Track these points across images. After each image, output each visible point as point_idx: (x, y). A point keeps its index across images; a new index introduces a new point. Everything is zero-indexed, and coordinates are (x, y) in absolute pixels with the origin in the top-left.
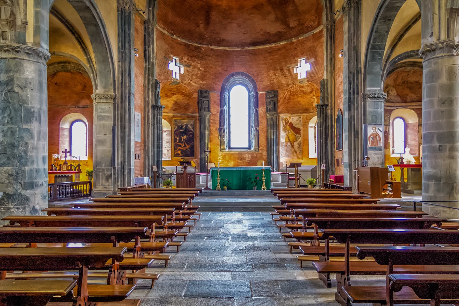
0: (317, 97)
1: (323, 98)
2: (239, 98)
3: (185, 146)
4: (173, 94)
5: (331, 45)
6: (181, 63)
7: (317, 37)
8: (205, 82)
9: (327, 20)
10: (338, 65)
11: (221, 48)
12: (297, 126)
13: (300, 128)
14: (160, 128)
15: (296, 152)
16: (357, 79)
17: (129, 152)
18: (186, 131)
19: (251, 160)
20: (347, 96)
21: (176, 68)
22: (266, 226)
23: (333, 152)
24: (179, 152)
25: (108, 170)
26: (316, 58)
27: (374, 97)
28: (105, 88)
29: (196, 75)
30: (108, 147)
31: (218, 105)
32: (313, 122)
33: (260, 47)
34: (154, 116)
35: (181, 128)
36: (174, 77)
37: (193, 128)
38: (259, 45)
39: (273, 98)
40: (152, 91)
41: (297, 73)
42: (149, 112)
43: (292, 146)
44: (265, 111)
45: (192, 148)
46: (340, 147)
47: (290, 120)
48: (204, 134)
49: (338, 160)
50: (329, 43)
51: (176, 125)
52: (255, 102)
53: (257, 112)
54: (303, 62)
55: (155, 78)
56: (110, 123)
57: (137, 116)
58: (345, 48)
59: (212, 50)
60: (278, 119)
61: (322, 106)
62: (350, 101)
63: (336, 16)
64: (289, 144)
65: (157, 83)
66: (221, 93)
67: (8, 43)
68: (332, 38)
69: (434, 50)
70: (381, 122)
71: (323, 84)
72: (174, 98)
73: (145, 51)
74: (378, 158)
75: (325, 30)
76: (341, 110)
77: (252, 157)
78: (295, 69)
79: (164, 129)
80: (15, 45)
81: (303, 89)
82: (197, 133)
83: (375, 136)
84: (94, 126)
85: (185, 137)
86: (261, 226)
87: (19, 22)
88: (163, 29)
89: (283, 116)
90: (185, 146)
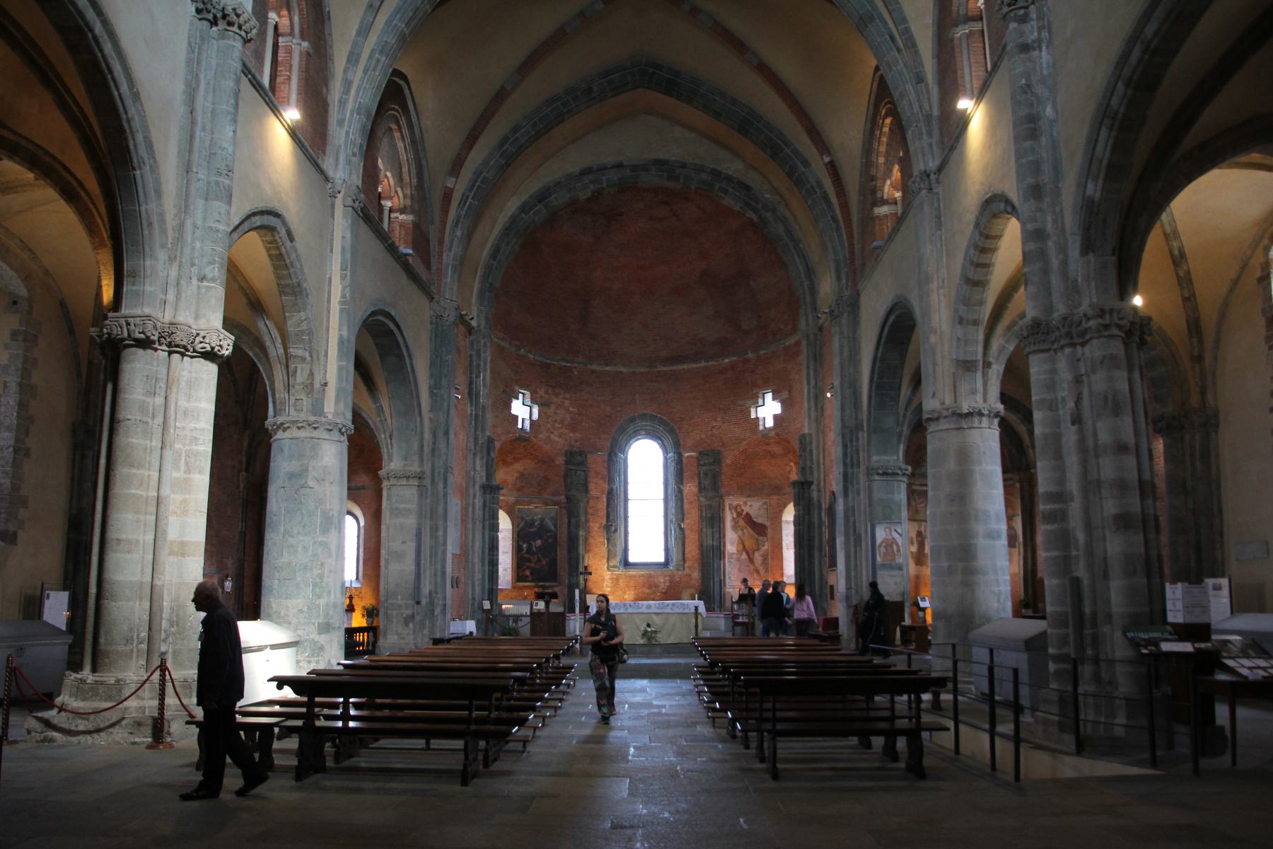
0: (796, 463)
1: (803, 469)
2: (645, 465)
3: (539, 560)
4: (516, 460)
5: (816, 371)
6: (534, 401)
7: (792, 353)
8: (578, 435)
9: (807, 325)
10: (828, 412)
11: (607, 368)
12: (759, 520)
13: (767, 523)
14: (494, 528)
15: (757, 571)
16: (857, 440)
17: (444, 573)
18: (542, 531)
19: (669, 588)
20: (841, 470)
21: (521, 410)
22: (684, 695)
23: (825, 572)
24: (528, 572)
25: (407, 607)
26: (790, 391)
27: (885, 474)
28: (405, 459)
29: (562, 422)
30: (409, 566)
31: (602, 478)
32: (789, 514)
33: (685, 366)
34: (484, 506)
35: (531, 524)
36: (520, 426)
37: (555, 526)
38: (683, 363)
39: (711, 464)
40: (482, 458)
41: (757, 418)
42: (474, 496)
43: (751, 560)
44: (695, 489)
45: (553, 563)
46: (833, 564)
47: (746, 509)
48: (577, 537)
49: (832, 587)
50: (812, 367)
51: (522, 518)
52: (677, 474)
53: (680, 491)
54: (769, 396)
55: (488, 433)
56: (411, 521)
57: (455, 505)
58: (837, 382)
59: (593, 372)
60: (720, 508)
61: (802, 484)
62: (846, 479)
63: (821, 321)
64: (744, 556)
65: (490, 441)
66: (609, 455)
67: (303, 416)
68: (818, 357)
69: (937, 419)
70: (900, 518)
71: (804, 441)
72: (518, 466)
73: (471, 384)
74: (896, 583)
75: (804, 343)
76: (833, 493)
77: (671, 581)
78: (753, 410)
79: (501, 527)
80: (312, 419)
81: (769, 448)
82: (563, 536)
83: (890, 543)
84: (383, 527)
85: (539, 542)
86: (677, 694)
87: (317, 385)
88: (503, 339)
89: (729, 501)
90: (539, 560)
